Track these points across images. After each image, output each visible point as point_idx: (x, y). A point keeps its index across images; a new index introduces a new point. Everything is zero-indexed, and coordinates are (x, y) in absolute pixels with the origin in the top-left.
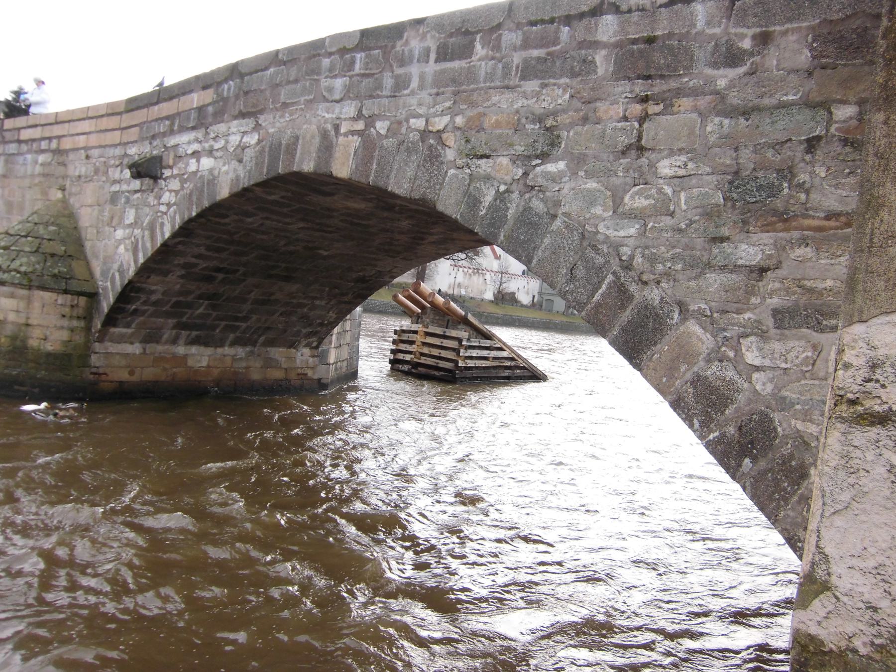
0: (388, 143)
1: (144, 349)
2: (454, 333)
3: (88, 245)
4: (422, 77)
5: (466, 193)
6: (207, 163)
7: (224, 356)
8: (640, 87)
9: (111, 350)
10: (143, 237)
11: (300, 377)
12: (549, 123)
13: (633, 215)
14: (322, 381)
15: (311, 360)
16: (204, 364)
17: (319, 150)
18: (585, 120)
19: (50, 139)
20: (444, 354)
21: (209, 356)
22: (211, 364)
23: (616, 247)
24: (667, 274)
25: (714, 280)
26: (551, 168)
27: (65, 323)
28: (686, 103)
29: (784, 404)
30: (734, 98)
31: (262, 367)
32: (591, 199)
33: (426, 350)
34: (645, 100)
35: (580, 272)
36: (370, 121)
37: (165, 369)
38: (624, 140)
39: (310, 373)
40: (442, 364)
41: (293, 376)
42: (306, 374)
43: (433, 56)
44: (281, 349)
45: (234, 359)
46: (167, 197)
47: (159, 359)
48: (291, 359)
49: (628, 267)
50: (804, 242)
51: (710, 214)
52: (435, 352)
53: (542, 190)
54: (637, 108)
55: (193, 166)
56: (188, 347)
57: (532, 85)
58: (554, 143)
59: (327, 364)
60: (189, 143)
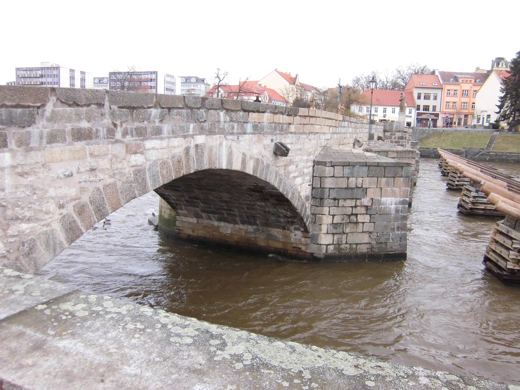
1: (198, 221)
7: (240, 229)
9: (184, 220)
11: (295, 249)
14: (314, 255)
15: (303, 239)
16: (229, 232)
21: (231, 228)
22: (233, 233)
31: (265, 239)
37: (208, 232)
39: (303, 248)
41: (289, 247)
42: (300, 248)
44: (278, 230)
45: (246, 232)
47: (205, 227)
48: (286, 237)
56: (219, 222)
59: (318, 244)
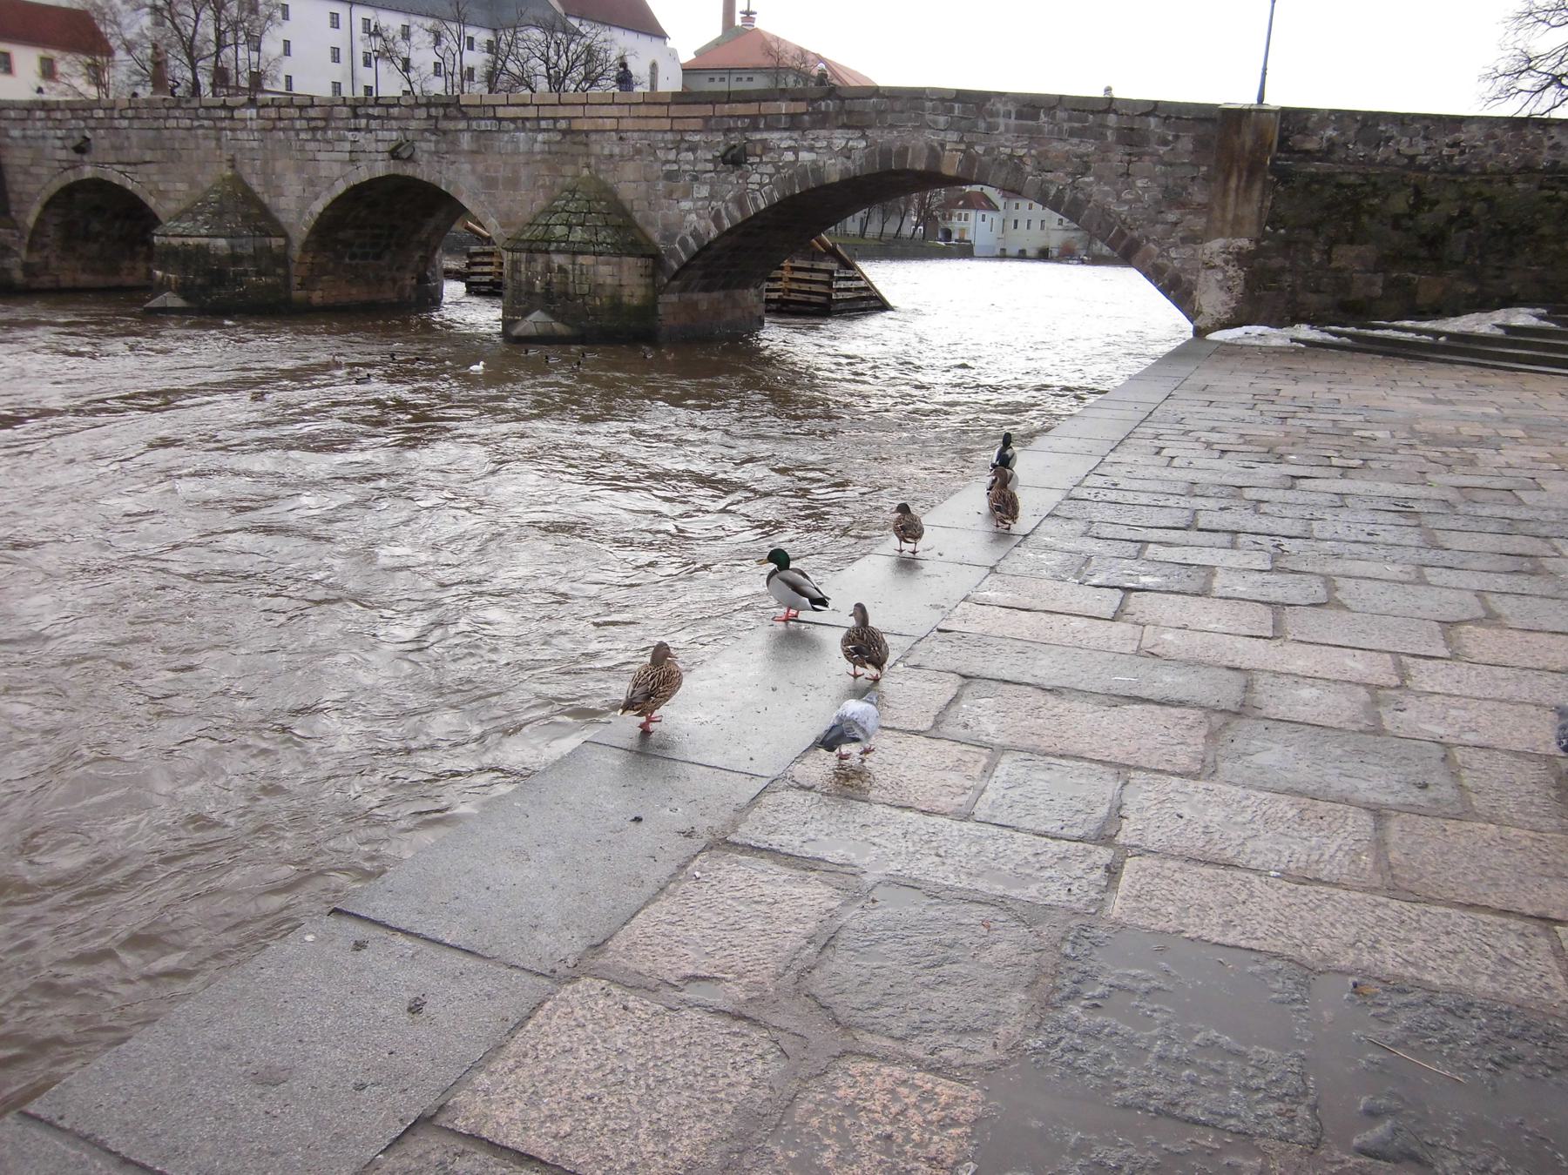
0: (986, 159)
2: (823, 266)
3: (637, 216)
4: (1006, 125)
5: (1041, 189)
6: (805, 156)
8: (1128, 149)
10: (726, 208)
12: (1085, 159)
13: (1126, 202)
17: (928, 157)
18: (1103, 160)
19: (555, 119)
20: (815, 288)
23: (1119, 215)
24: (1141, 226)
25: (1159, 227)
26: (1086, 179)
27: (642, 281)
28: (1147, 158)
29: (1185, 270)
30: (1166, 159)
32: (1106, 194)
33: (794, 286)
34: (1130, 154)
35: (1103, 225)
36: (970, 145)
38: (1121, 171)
40: (814, 299)
43: (1013, 116)
46: (755, 178)
49: (1124, 222)
50: (1190, 213)
51: (1157, 202)
52: (805, 287)
53: (1082, 189)
54: (1127, 158)
55: (789, 156)
57: (1075, 140)
58: (1088, 168)
60: (781, 139)
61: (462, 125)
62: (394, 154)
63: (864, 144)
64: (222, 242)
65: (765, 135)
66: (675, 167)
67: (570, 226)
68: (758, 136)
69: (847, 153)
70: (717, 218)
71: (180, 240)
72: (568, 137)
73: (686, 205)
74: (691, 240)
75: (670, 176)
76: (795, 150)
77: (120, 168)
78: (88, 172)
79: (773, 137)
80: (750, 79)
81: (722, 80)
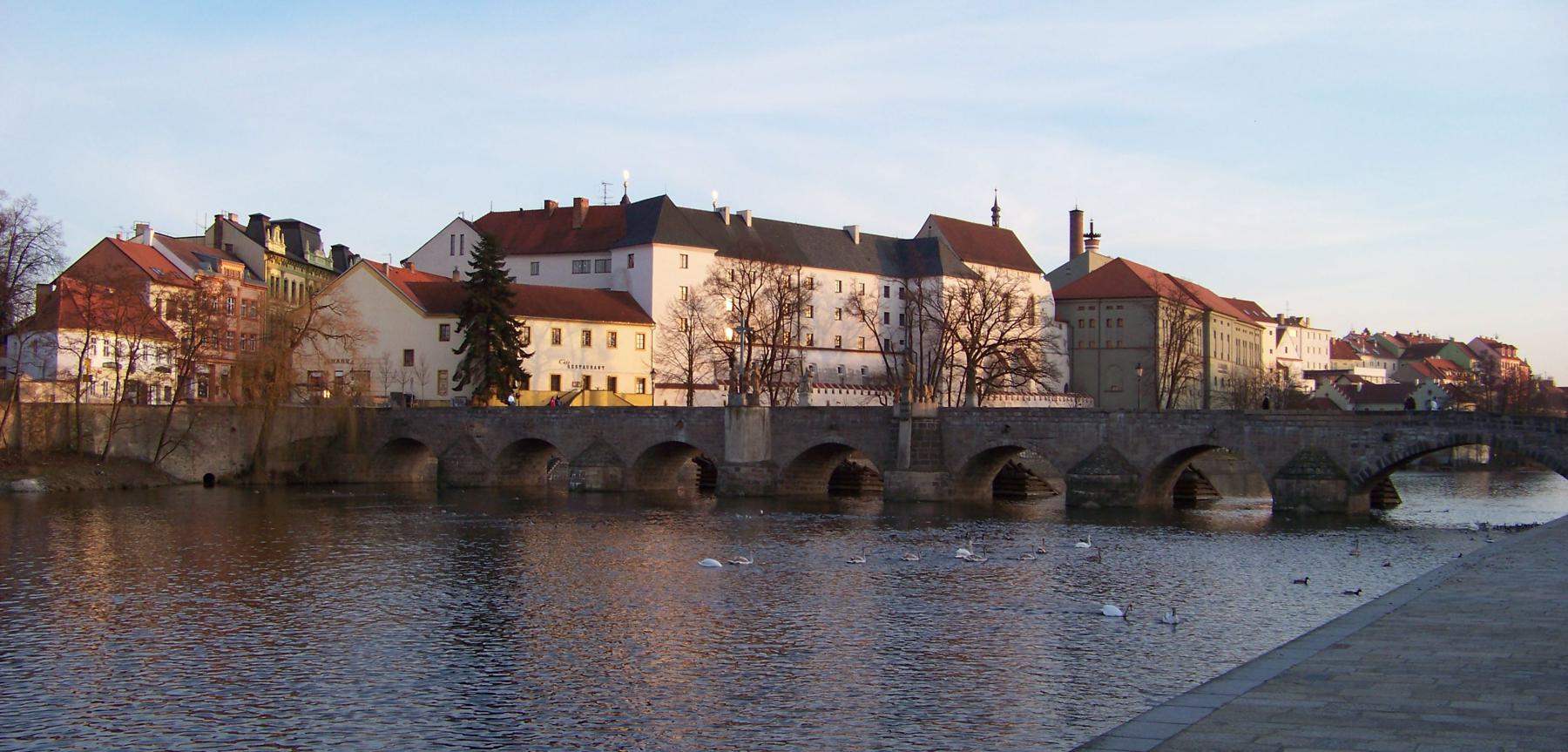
6: (1421, 438)
10: (1384, 460)
55: (1413, 438)
61: (1245, 423)
62: (1210, 435)
63: (1447, 433)
64: (1117, 477)
65: (1402, 429)
66: (1356, 442)
67: (1315, 469)
68: (1397, 430)
69: (1439, 436)
70: (1378, 463)
71: (1097, 476)
72: (1303, 429)
73: (1363, 458)
74: (1365, 473)
75: (1354, 445)
76: (1416, 435)
77: (1030, 440)
78: (1006, 442)
79: (1405, 430)
80: (1119, 307)
81: (1092, 308)
